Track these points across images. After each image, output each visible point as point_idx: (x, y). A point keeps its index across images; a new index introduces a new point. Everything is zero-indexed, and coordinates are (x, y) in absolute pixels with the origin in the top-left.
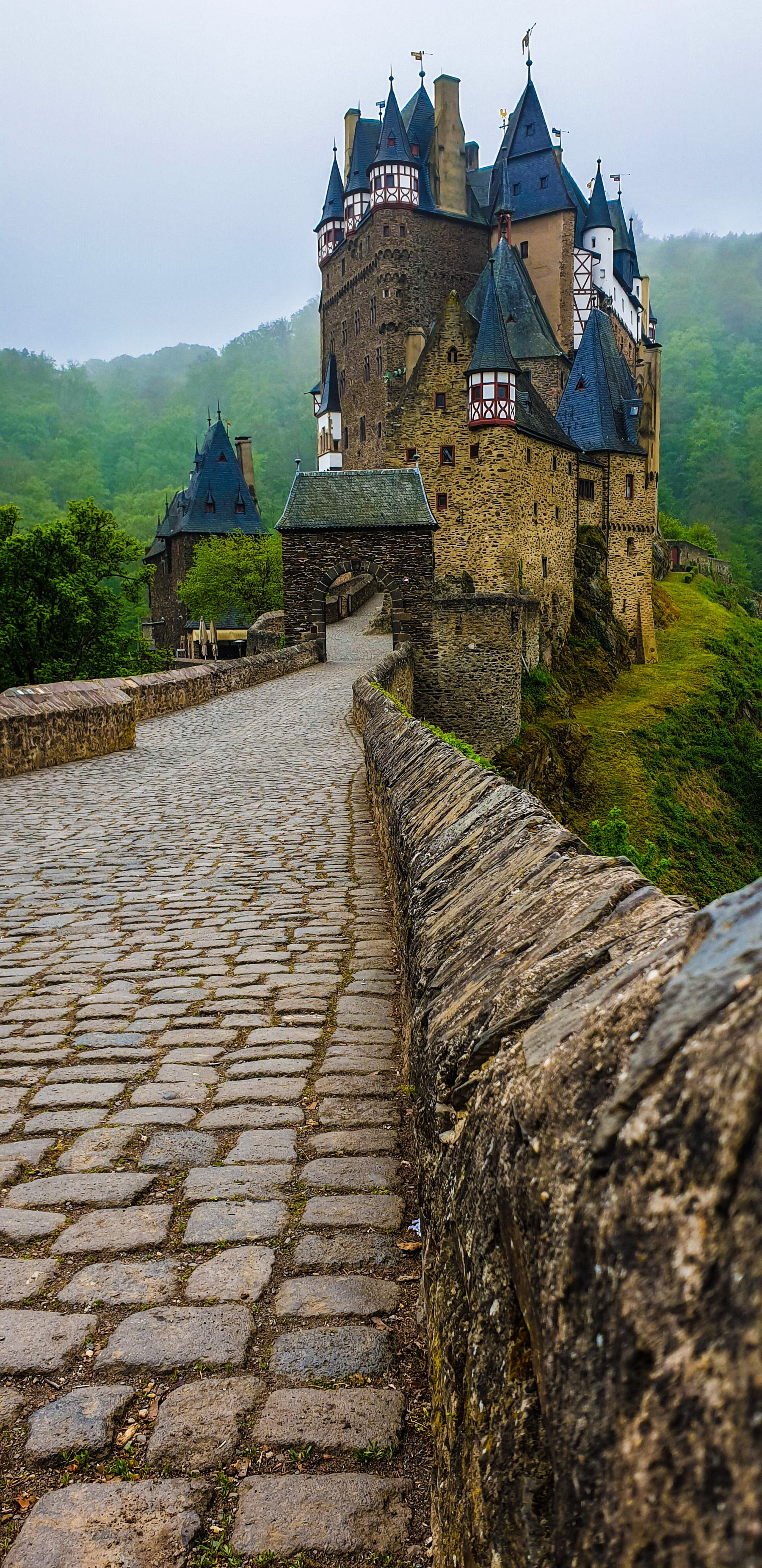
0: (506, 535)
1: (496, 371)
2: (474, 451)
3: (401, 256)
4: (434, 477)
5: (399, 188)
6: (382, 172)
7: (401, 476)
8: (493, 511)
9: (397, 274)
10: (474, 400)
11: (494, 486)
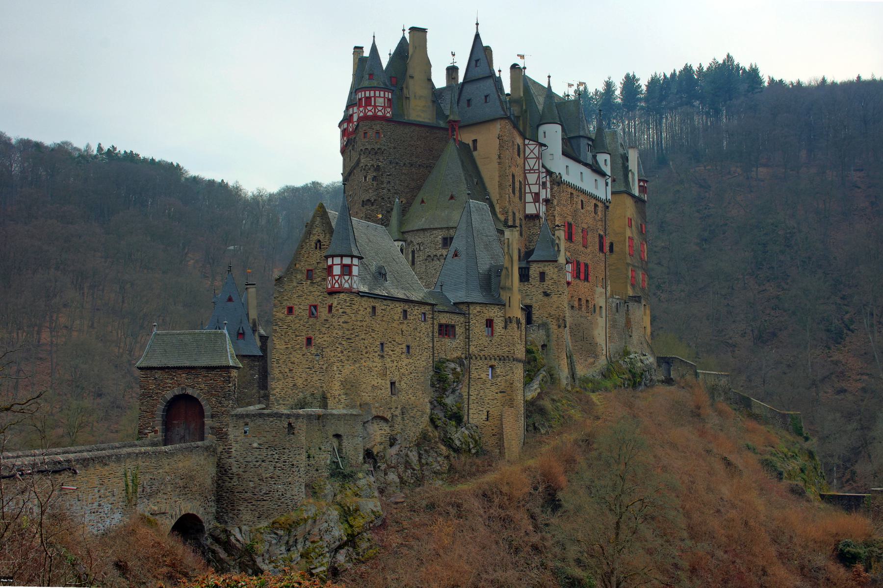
0: (348, 366)
1: (342, 256)
2: (330, 308)
3: (376, 153)
4: (304, 326)
5: (375, 107)
6: (363, 96)
7: (215, 334)
8: (339, 350)
9: (373, 165)
11: (340, 333)
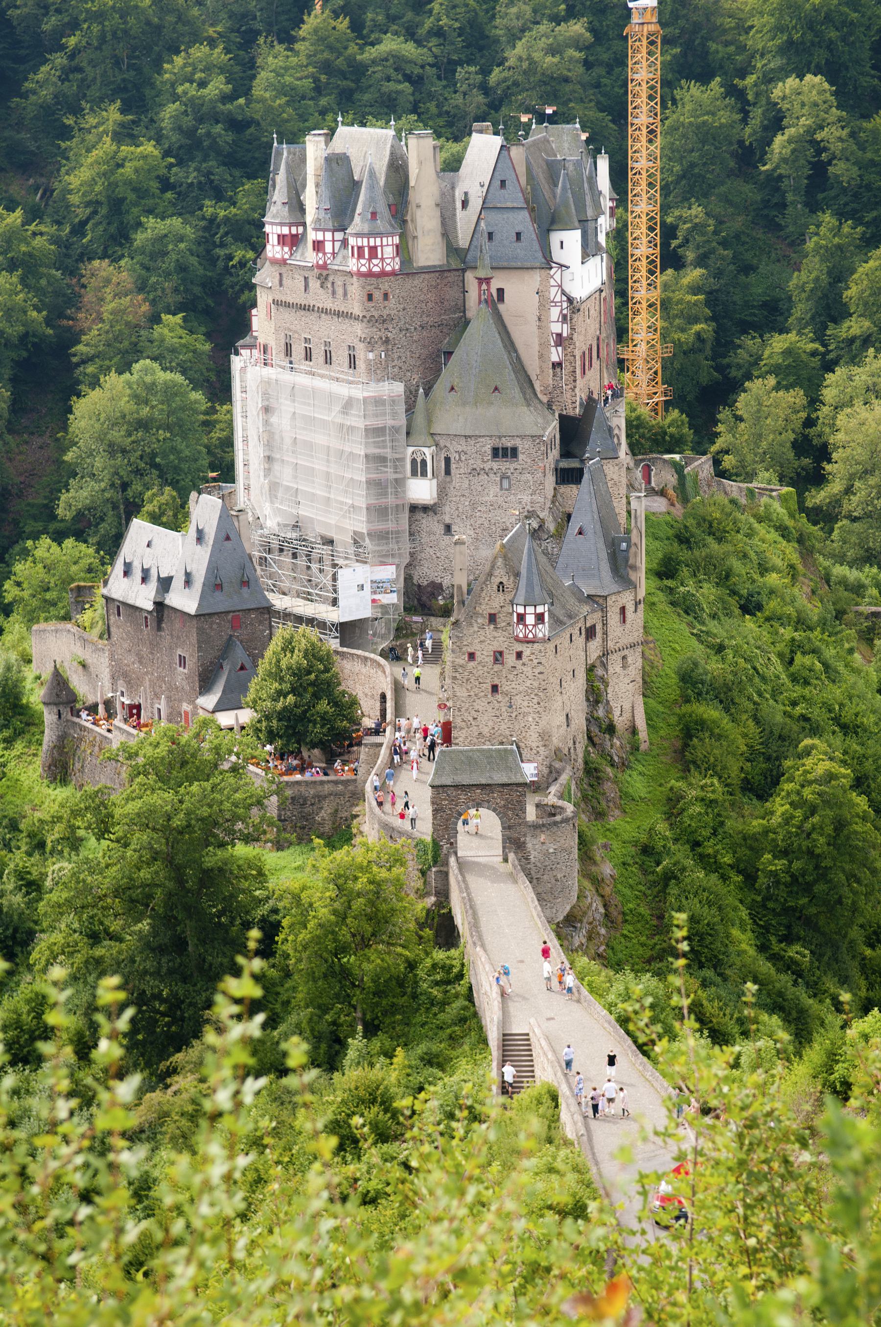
2: (519, 655)
5: (382, 259)
6: (365, 243)
7: (506, 750)
10: (518, 623)
